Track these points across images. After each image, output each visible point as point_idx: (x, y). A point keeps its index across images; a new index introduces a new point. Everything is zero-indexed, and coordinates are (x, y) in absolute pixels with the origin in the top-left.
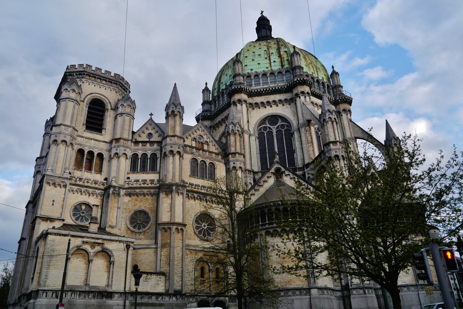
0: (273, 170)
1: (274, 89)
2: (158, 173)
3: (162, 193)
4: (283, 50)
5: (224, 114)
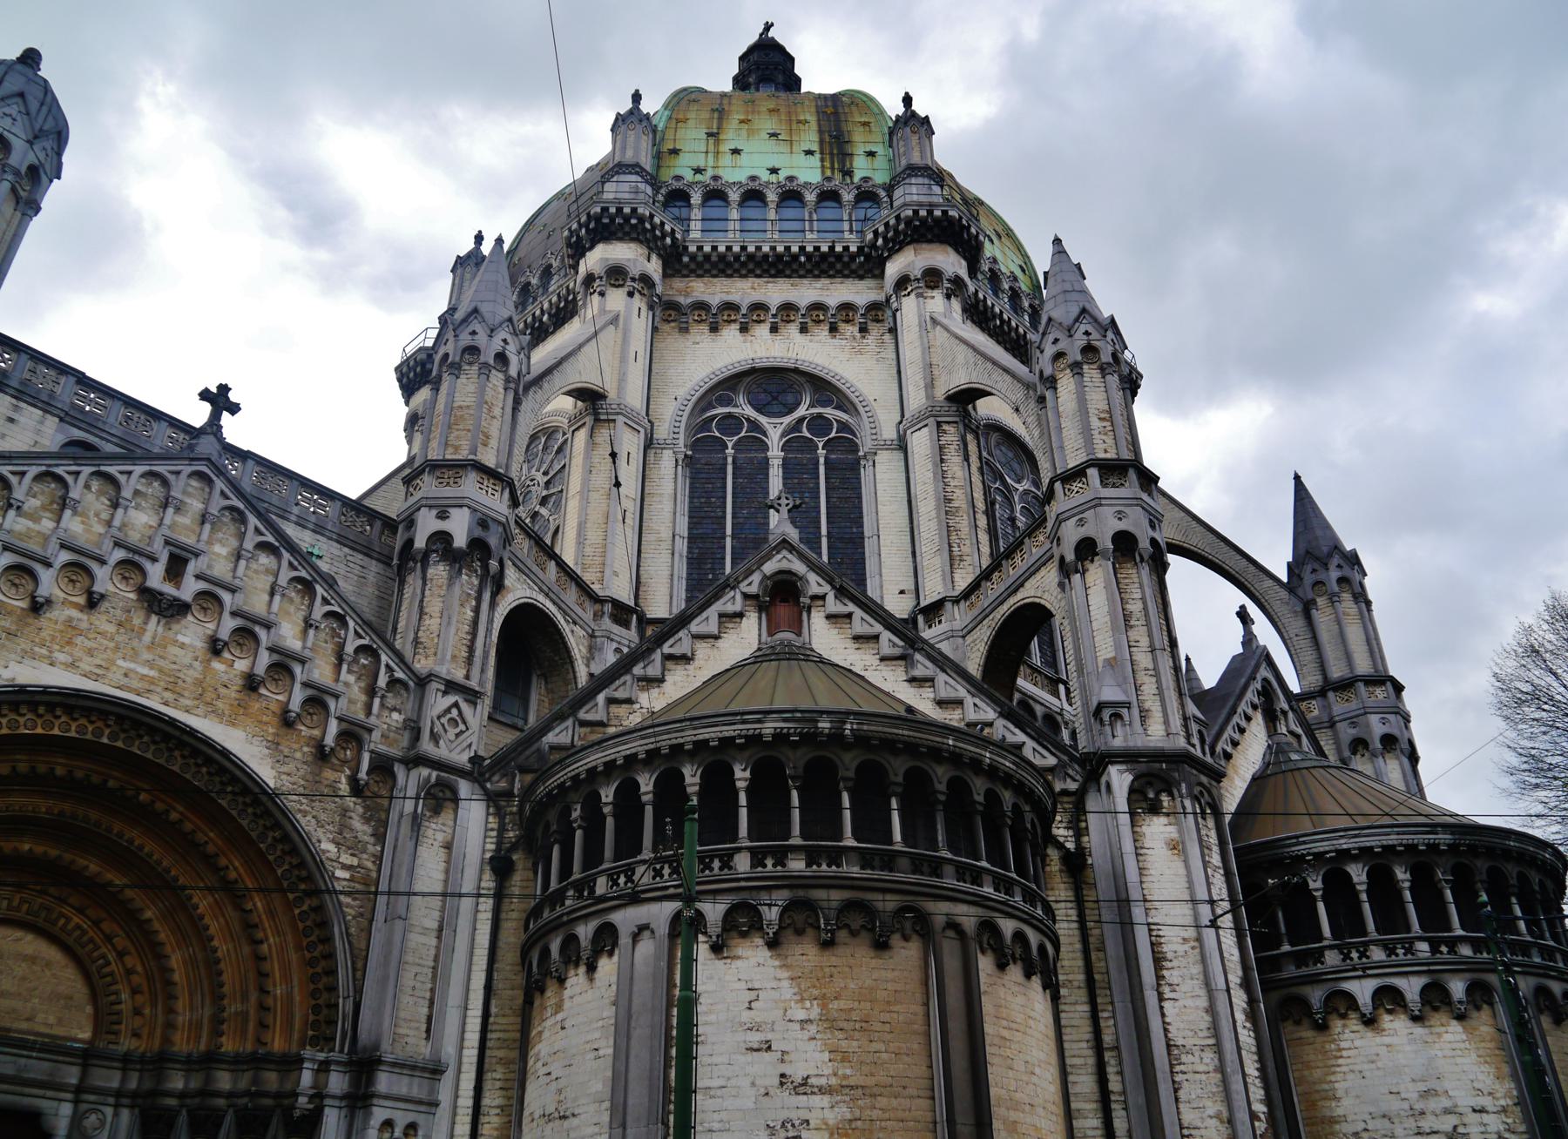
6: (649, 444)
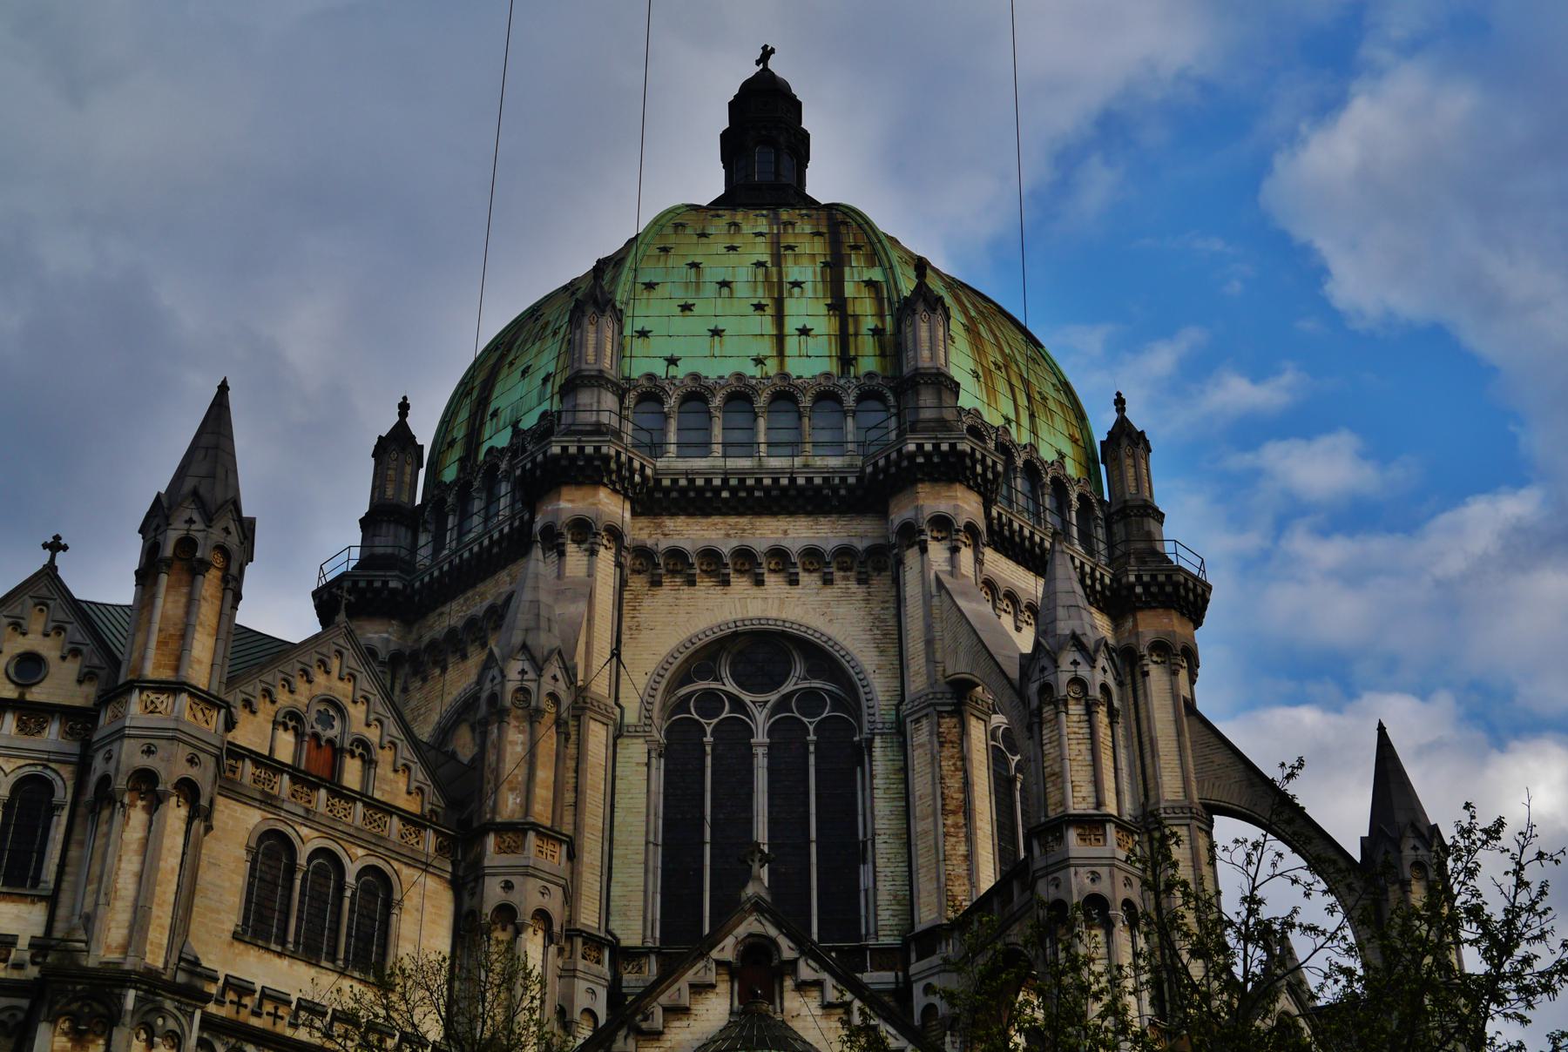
0: (727, 950)
1: (784, 482)
2: (41, 898)
3: (53, 1021)
4: (856, 274)
5: (482, 595)
6: (619, 732)
